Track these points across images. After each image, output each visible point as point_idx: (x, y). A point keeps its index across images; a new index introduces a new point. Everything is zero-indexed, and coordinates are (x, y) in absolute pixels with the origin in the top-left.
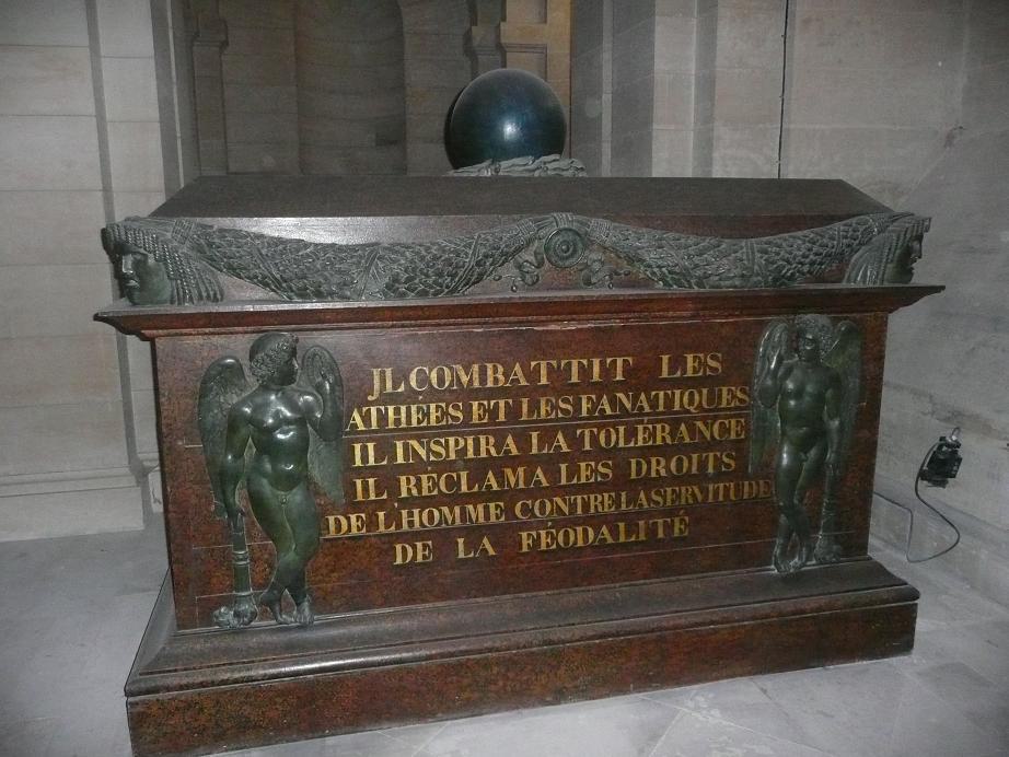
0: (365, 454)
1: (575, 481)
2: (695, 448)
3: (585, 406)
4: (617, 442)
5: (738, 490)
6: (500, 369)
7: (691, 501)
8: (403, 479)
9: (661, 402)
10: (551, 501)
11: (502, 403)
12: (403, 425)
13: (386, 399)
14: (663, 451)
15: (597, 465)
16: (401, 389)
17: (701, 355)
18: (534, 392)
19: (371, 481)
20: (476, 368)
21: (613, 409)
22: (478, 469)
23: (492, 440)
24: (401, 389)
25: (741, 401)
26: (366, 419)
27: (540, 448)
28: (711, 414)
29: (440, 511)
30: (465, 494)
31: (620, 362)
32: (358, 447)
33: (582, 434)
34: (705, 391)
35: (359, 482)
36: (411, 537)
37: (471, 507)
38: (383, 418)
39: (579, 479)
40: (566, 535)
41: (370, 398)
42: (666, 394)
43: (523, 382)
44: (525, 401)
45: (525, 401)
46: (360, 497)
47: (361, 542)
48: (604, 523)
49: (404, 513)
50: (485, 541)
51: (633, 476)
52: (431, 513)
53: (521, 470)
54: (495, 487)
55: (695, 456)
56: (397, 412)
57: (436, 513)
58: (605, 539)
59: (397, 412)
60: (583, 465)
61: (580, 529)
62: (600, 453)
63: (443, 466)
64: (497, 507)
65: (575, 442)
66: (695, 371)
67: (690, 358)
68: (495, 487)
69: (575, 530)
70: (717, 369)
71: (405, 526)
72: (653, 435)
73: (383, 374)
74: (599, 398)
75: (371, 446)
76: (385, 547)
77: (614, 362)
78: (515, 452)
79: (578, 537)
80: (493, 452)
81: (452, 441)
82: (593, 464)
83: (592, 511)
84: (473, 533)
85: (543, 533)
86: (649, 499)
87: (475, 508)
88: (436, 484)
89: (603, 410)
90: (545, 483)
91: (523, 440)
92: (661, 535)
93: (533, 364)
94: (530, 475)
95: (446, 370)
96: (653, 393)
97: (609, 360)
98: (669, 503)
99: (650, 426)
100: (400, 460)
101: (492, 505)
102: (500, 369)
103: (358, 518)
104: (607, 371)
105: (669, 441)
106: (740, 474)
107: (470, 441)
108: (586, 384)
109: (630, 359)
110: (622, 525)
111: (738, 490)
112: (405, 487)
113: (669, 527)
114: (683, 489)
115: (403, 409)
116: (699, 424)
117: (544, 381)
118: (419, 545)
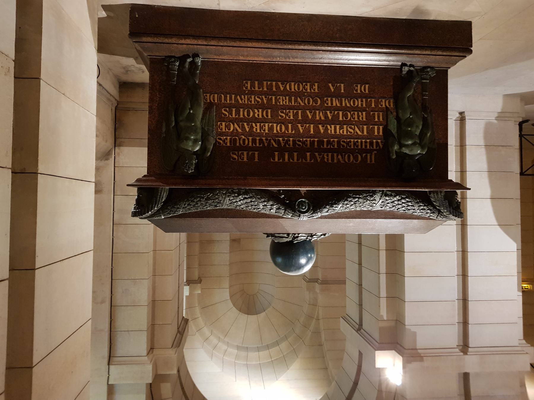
0: (378, 131)
1: (295, 111)
2: (242, 120)
3: (291, 143)
4: (277, 126)
5: (220, 99)
6: (326, 160)
7: (243, 96)
8: (364, 119)
9: (258, 141)
10: (305, 104)
11: (325, 146)
12: (364, 140)
13: (370, 151)
14: (256, 120)
15: (286, 117)
16: (364, 155)
17: (240, 160)
18: (312, 149)
19: (376, 120)
20: (335, 161)
21: (279, 140)
22: (335, 121)
23: (329, 132)
24: (364, 155)
25: (221, 139)
26: (377, 143)
27: (309, 127)
28: (235, 133)
29: (350, 105)
30: (340, 111)
31: (276, 160)
32: (381, 133)
33: (292, 131)
34: (238, 144)
35: (381, 120)
36: (362, 96)
37: (338, 105)
38: (371, 144)
39: (293, 112)
40: (299, 88)
41: (376, 152)
42: (256, 145)
43: (317, 154)
44: (316, 147)
45: (316, 147)
46: (381, 113)
47: (382, 95)
48: (282, 91)
49: (364, 106)
50: (333, 90)
51: (269, 111)
52: (354, 105)
53: (318, 118)
54: (328, 112)
55: (242, 116)
56: (366, 146)
57: (352, 104)
58: (282, 84)
59: (366, 146)
60: (292, 118)
61: (293, 90)
62: (283, 122)
63: (349, 123)
64: (328, 104)
65: (295, 128)
66: (243, 154)
67: (245, 159)
68: (328, 112)
69: (295, 90)
70: (233, 154)
71: (364, 100)
72: (261, 128)
73: (371, 161)
74: (285, 145)
75: (376, 134)
76: (372, 92)
77: (279, 160)
78: (320, 126)
79: (294, 87)
80: (329, 127)
81: (345, 133)
82: (287, 118)
83: (287, 98)
84: (338, 95)
85: (309, 91)
86: (262, 99)
87: (336, 104)
88: (352, 116)
89: (283, 140)
90: (308, 112)
91: (317, 130)
92: (256, 83)
93: (312, 161)
94: (314, 115)
95: (347, 161)
96: (261, 145)
97: (281, 161)
98: (253, 97)
99: (262, 131)
100: (365, 127)
101: (330, 105)
102: (326, 160)
103: (382, 106)
104: (282, 156)
105: (254, 125)
106: (220, 106)
107: (338, 133)
108: (291, 153)
109: (272, 160)
110: (274, 89)
111: (220, 99)
112: (363, 116)
113: (253, 85)
114: (246, 102)
115: (364, 147)
116: (240, 131)
117: (308, 154)
118: (359, 92)
